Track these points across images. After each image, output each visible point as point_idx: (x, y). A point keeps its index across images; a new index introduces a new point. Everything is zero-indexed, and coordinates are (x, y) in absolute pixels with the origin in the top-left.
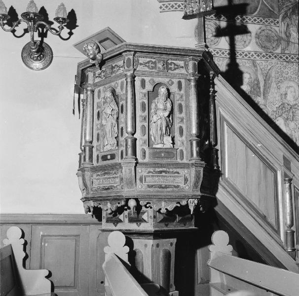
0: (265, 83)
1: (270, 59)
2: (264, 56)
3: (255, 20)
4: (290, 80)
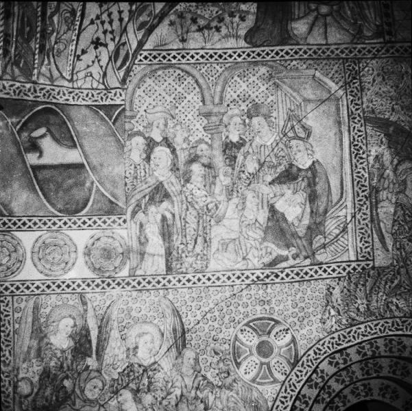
0: (100, 332)
1: (108, 289)
2: (98, 286)
3: (84, 223)
4: (145, 322)
